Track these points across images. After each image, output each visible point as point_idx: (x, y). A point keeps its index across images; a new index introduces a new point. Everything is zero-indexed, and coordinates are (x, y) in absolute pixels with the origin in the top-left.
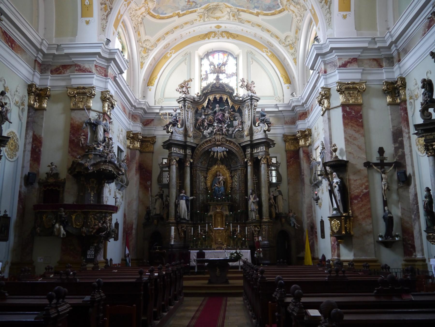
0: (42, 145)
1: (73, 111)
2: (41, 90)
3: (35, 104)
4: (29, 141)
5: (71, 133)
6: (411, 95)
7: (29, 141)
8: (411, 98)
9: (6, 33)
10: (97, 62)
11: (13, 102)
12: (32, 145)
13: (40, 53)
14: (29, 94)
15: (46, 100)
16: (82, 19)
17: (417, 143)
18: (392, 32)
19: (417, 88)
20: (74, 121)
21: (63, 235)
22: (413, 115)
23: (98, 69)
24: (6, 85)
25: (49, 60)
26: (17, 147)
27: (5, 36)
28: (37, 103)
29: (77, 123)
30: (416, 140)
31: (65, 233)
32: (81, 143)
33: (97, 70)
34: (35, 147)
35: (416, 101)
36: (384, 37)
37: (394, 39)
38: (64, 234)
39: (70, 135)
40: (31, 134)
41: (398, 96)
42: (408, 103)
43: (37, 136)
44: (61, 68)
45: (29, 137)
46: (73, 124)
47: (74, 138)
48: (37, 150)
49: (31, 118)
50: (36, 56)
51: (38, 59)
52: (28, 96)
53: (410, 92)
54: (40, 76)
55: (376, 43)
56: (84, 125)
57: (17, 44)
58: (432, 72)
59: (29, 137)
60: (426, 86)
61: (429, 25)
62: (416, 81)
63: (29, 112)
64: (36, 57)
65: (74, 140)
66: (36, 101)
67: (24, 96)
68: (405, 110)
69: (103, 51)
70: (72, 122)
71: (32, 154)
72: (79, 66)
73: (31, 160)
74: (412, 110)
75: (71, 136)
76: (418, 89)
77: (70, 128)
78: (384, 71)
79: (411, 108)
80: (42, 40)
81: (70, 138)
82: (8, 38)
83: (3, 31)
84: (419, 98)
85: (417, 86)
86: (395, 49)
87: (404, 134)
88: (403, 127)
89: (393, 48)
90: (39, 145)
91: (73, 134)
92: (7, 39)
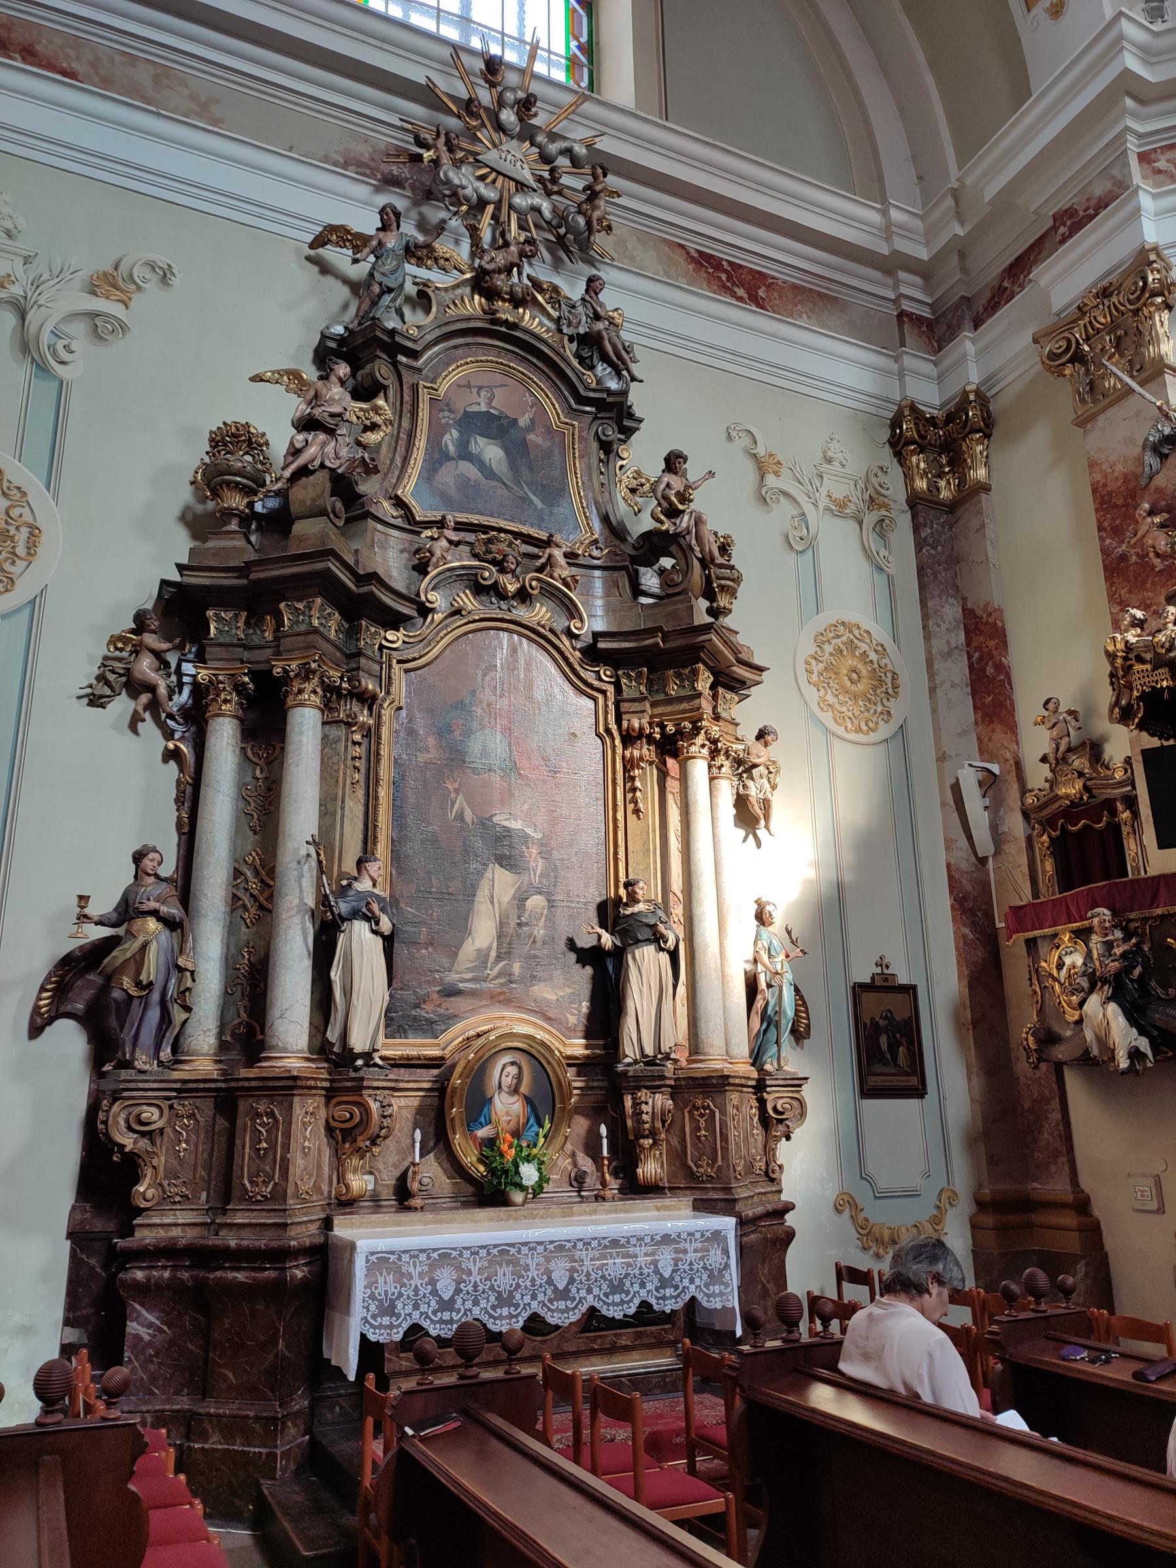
0: (1005, 644)
1: (1089, 426)
2: (950, 418)
3: (942, 483)
4: (948, 642)
5: (1105, 530)
7: (948, 642)
9: (712, 256)
10: (1140, 136)
11: (815, 505)
12: (970, 657)
13: (902, 275)
14: (898, 455)
15: (979, 448)
16: (1034, 12)
20: (1105, 467)
21: (1135, 1054)
23: (1162, 164)
24: (761, 451)
25: (951, 279)
26: (889, 680)
27: (711, 270)
28: (948, 483)
29: (1119, 468)
31: (1144, 1044)
32: (1152, 555)
33: (1159, 171)
34: (980, 659)
38: (1137, 1049)
39: (1102, 540)
40: (951, 611)
43: (979, 612)
44: (1006, 284)
45: (944, 627)
46: (1105, 485)
47: (1124, 547)
48: (990, 670)
49: (935, 548)
50: (892, 296)
51: (907, 306)
52: (902, 466)
54: (935, 364)
56: (1150, 459)
57: (780, 282)
59: (944, 627)
63: (916, 529)
64: (896, 301)
65: (1124, 557)
66: (940, 476)
67: (876, 470)
69: (1148, 55)
70: (1098, 477)
71: (974, 694)
72: (1070, 212)
73: (976, 723)
75: (1108, 542)
77: (1097, 510)
80: (884, 213)
81: (1105, 552)
82: (726, 271)
83: (695, 255)
90: (992, 643)
91: (1117, 532)
92: (724, 277)
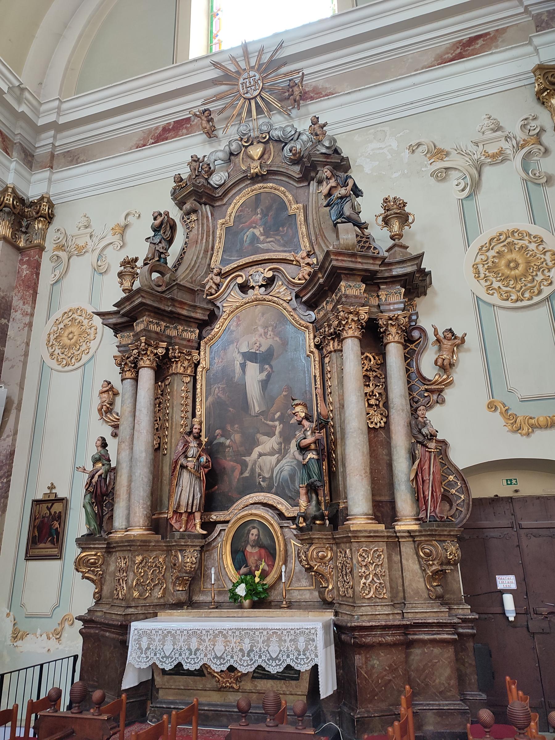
6: (64, 242)
8: (61, 248)
17: (51, 340)
18: (65, 106)
19: (89, 235)
22: (56, 282)
30: (49, 334)
35: (74, 259)
36: (41, 104)
37: (62, 121)
41: (26, 233)
42: (46, 257)
53: (62, 237)
55: (19, 101)
58: (141, 216)
60: (166, 226)
61: (160, 135)
62: (89, 221)
68: (36, 267)
74: (57, 272)
76: (91, 236)
78: (13, 165)
79: (55, 269)
84: (87, 254)
85: (89, 230)
86: (51, 140)
87: (16, 315)
88: (15, 299)
89: (46, 139)
